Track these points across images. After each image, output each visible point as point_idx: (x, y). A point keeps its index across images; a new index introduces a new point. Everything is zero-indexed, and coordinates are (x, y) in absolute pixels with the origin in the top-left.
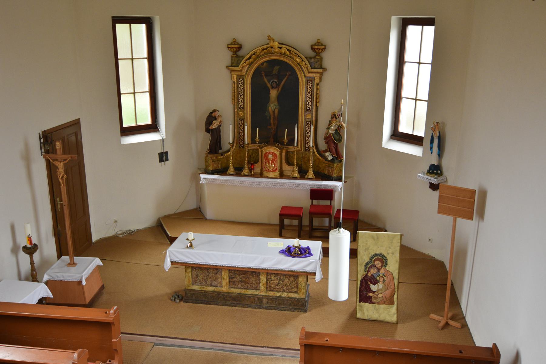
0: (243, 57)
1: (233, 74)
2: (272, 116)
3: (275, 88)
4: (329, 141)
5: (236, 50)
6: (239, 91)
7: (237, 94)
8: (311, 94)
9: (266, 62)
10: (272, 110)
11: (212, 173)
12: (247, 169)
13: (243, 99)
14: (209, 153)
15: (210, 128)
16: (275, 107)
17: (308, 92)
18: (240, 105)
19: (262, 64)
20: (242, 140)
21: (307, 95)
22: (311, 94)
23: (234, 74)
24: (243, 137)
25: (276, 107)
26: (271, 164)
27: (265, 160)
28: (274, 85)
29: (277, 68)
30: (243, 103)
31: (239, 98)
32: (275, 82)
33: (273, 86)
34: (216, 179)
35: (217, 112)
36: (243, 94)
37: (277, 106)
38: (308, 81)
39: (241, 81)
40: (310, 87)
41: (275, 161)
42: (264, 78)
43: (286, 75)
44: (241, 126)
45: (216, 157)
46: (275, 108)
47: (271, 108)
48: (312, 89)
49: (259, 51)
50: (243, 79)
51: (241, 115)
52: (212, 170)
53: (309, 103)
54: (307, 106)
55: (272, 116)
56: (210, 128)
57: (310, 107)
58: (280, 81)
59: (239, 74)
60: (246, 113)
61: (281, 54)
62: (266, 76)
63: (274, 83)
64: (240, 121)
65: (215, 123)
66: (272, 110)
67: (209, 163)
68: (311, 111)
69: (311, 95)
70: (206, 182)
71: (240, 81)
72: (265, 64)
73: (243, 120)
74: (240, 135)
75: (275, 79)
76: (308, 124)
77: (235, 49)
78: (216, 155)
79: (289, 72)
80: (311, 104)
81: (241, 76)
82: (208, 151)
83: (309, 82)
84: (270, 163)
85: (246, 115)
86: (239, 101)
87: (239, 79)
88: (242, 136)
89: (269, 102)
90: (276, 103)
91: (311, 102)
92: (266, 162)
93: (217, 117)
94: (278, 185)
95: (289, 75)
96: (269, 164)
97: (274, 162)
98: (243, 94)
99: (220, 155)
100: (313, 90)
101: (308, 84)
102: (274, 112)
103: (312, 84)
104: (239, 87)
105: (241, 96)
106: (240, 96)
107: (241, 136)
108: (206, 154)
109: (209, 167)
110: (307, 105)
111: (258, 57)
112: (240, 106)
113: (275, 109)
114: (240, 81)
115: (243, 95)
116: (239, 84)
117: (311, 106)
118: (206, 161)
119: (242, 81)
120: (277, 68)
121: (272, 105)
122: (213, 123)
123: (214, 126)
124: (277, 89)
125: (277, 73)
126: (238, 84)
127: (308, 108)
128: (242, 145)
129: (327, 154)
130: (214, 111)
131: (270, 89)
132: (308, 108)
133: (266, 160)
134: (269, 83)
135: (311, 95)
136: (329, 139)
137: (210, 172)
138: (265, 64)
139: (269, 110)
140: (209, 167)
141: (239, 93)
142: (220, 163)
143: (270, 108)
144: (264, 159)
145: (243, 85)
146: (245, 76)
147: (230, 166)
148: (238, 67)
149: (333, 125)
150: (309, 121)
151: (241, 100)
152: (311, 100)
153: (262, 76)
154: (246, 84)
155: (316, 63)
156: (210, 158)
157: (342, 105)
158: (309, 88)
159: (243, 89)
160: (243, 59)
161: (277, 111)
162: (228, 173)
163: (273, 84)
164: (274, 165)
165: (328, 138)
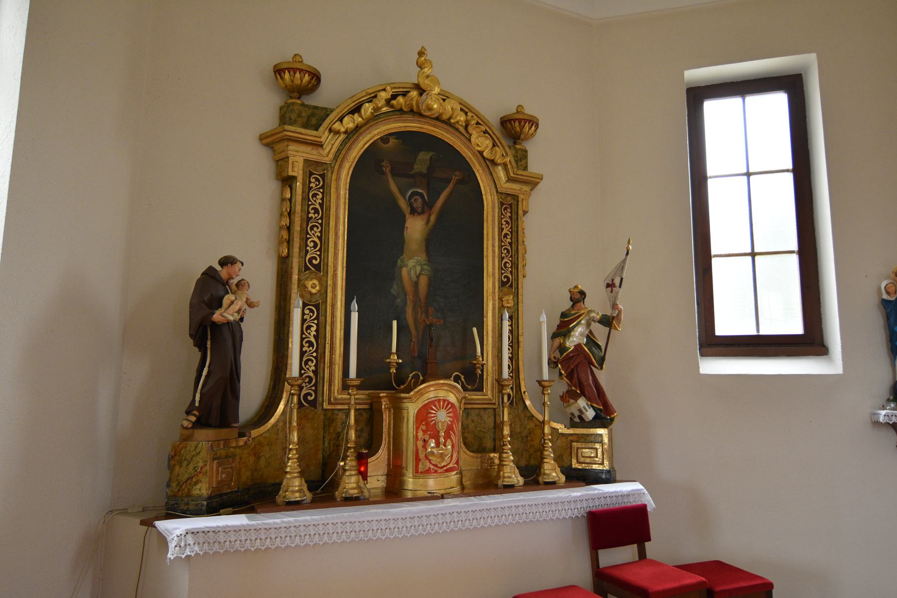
0: (327, 112)
1: (293, 153)
2: (410, 298)
3: (419, 214)
4: (577, 366)
5: (309, 82)
6: (309, 213)
7: (302, 220)
8: (510, 241)
9: (399, 135)
10: (410, 279)
11: (212, 510)
12: (353, 473)
13: (320, 238)
15: (217, 317)
16: (418, 269)
17: (503, 233)
18: (308, 257)
19: (385, 139)
20: (309, 377)
21: (502, 241)
22: (510, 241)
23: (294, 156)
24: (316, 366)
25: (422, 270)
26: (445, 445)
27: (420, 434)
28: (418, 204)
29: (424, 156)
30: (320, 250)
31: (308, 233)
32: (421, 195)
33: (415, 205)
34: (247, 530)
36: (320, 221)
37: (425, 267)
38: (502, 204)
39: (317, 179)
41: (454, 434)
42: (388, 181)
43: (448, 181)
46: (420, 274)
47: (409, 272)
48: (511, 228)
49: (384, 95)
50: (323, 176)
51: (314, 291)
52: (210, 498)
53: (507, 265)
54: (502, 274)
55: (411, 297)
56: (217, 317)
57: (510, 276)
58: (434, 195)
59: (313, 154)
60: (330, 282)
61: (438, 119)
62: (394, 174)
63: (418, 197)
65: (232, 302)
66: (410, 279)
67: (201, 464)
68: (511, 286)
69: (510, 244)
70: (196, 548)
71: (313, 180)
72: (393, 141)
73: (317, 306)
74: (304, 359)
75: (420, 188)
78: (224, 432)
79: (457, 173)
80: (511, 267)
81: (318, 164)
82: (193, 419)
83: (506, 209)
84: (442, 440)
85: (329, 289)
86: (307, 245)
87: (311, 174)
89: (401, 251)
90: (422, 257)
91: (511, 261)
92: (427, 437)
93: (234, 287)
94: (485, 515)
95: (459, 182)
96: (438, 444)
97: (453, 437)
98: (320, 221)
99: (235, 432)
100: (514, 229)
101: (502, 214)
102: (416, 285)
103: (511, 213)
104: (309, 200)
105: (315, 229)
106: (312, 229)
108: (186, 428)
109: (196, 483)
110: (502, 269)
111: (376, 117)
112: (310, 260)
113: (418, 277)
114: (313, 180)
115: (321, 224)
116: (310, 188)
117: (511, 272)
118: (175, 458)
119: (319, 183)
120: (424, 156)
121: (411, 263)
123: (225, 314)
124: (425, 217)
125: (425, 171)
126: (307, 188)
127: (505, 280)
128: (311, 395)
129: (582, 402)
130: (227, 261)
131: (407, 215)
132: (505, 277)
133: (425, 432)
134: (403, 195)
135: (510, 244)
136: (578, 360)
137: (205, 503)
138: (393, 141)
139: (401, 278)
140: (198, 487)
141: (309, 219)
143: (404, 271)
145: (323, 193)
148: (317, 130)
149: (583, 322)
151: (314, 241)
152: (511, 256)
153: (383, 173)
154: (333, 190)
156: (204, 446)
157: (627, 254)
158: (504, 223)
159: (321, 205)
160: (327, 115)
161: (423, 282)
162: (279, 499)
163: (415, 200)
164: (453, 446)
165: (572, 357)
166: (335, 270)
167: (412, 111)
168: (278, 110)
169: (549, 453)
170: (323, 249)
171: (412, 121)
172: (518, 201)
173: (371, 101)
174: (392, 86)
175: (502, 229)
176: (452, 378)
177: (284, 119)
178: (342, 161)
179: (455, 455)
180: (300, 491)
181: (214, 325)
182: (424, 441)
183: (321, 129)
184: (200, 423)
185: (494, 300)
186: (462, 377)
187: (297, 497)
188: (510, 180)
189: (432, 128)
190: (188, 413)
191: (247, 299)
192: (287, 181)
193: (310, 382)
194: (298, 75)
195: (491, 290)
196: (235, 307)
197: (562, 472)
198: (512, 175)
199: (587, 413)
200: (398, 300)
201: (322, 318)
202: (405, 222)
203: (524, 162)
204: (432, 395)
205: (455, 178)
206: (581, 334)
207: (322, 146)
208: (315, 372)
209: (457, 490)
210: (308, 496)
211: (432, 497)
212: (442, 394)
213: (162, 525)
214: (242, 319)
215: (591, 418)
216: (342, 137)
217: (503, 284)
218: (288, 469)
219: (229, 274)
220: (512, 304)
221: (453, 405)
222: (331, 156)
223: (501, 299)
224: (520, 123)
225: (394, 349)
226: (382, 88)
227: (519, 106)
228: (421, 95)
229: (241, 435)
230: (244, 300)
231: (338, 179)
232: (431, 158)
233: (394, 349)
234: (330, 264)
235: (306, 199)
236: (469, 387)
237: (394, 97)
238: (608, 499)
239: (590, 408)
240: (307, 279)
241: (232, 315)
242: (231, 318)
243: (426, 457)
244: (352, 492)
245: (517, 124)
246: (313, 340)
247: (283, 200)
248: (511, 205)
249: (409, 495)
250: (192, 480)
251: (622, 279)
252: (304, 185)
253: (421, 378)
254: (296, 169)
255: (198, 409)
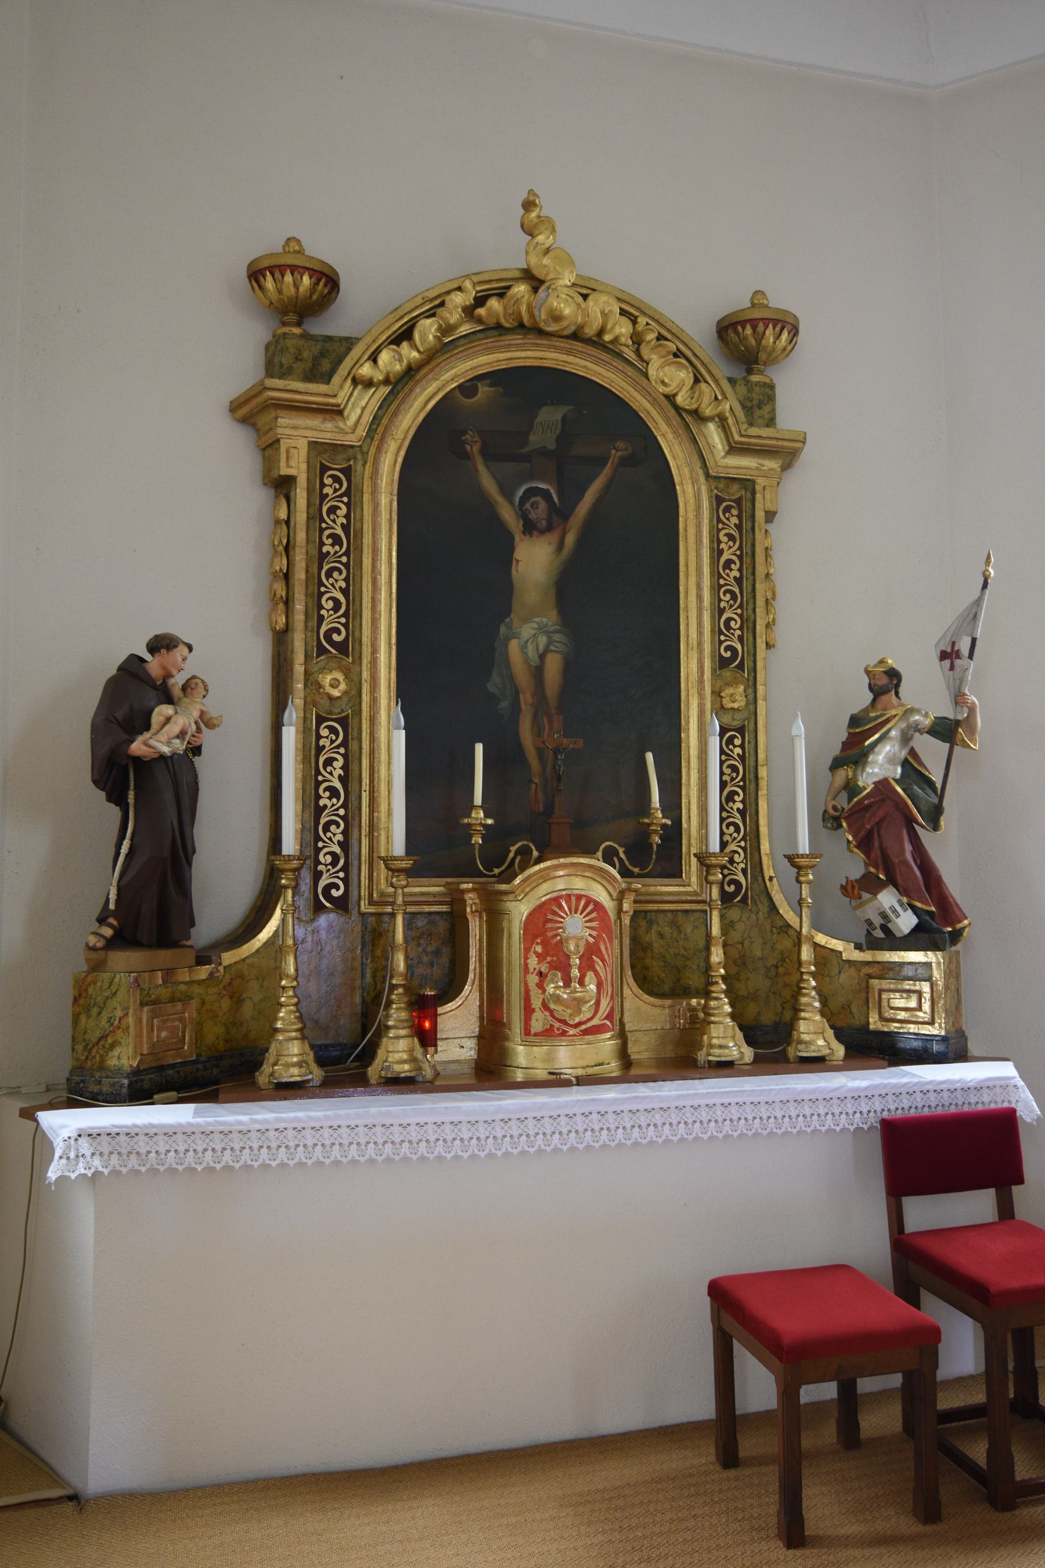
0: (349, 343)
1: (288, 431)
2: (526, 699)
3: (542, 532)
4: (879, 824)
5: (313, 289)
6: (322, 544)
7: (309, 559)
8: (738, 575)
9: (495, 377)
12: (403, 1032)
13: (345, 592)
14: (111, 944)
15: (137, 747)
16: (543, 640)
17: (723, 560)
18: (324, 628)
19: (468, 388)
21: (720, 576)
22: (738, 575)
23: (289, 437)
24: (345, 833)
25: (550, 642)
26: (581, 983)
27: (533, 962)
28: (539, 511)
29: (550, 416)
30: (346, 615)
31: (321, 584)
32: (546, 495)
33: (533, 515)
34: (188, 1132)
35: (183, 650)
36: (344, 559)
37: (557, 637)
38: (719, 500)
40: (731, 537)
41: (603, 960)
42: (477, 471)
43: (602, 461)
44: (329, 762)
45: (169, 973)
46: (547, 650)
47: (523, 648)
48: (740, 548)
49: (458, 300)
50: (347, 472)
51: (336, 693)
52: (136, 1072)
53: (732, 623)
54: (721, 642)
55: (530, 699)
56: (137, 747)
57: (739, 647)
58: (572, 494)
59: (325, 430)
60: (365, 675)
61: (576, 336)
62: (488, 456)
63: (538, 499)
64: (324, 732)
65: (168, 720)
66: (526, 661)
67: (119, 1013)
69: (739, 581)
70: (97, 1162)
71: (328, 481)
72: (484, 391)
73: (344, 722)
74: (323, 820)
75: (544, 480)
76: (733, 737)
77: (306, 279)
78: (164, 956)
79: (619, 444)
80: (741, 628)
81: (335, 448)
82: (108, 932)
83: (727, 509)
84: (575, 972)
86: (321, 607)
87: (324, 469)
88: (337, 833)
89: (506, 610)
90: (550, 618)
91: (741, 616)
92: (544, 968)
93: (177, 692)
94: (658, 1119)
95: (624, 462)
96: (567, 983)
97: (599, 966)
98: (344, 559)
99: (190, 957)
100: (747, 549)
101: (719, 520)
102: (538, 673)
103: (739, 516)
104: (322, 520)
105: (335, 574)
106: (329, 574)
107: (326, 828)
108: (93, 949)
109: (112, 1046)
110: (721, 633)
112: (328, 635)
113: (542, 657)
114: (328, 481)
115: (347, 565)
116: (323, 497)
117: (741, 639)
119: (341, 485)
120: (550, 416)
121: (527, 631)
122: (156, 718)
124: (553, 537)
125: (552, 446)
127: (728, 654)
129: (888, 898)
130: (161, 644)
131: (517, 538)
132: (727, 649)
133: (541, 957)
134: (508, 496)
135: (739, 581)
136: (881, 813)
137: (126, 1082)
138: (484, 391)
139: (507, 662)
140: (116, 1052)
141: (323, 557)
142: (190, 1013)
143: (514, 645)
144: (527, 950)
146: (365, 454)
147: (279, 1025)
148: (328, 382)
149: (893, 733)
150: (736, 723)
152: (741, 606)
153: (466, 456)
154: (366, 497)
155: (759, 407)
156: (123, 980)
157: (985, 586)
158: (725, 539)
159: (346, 528)
161: (553, 666)
162: (262, 1078)
163: (532, 506)
164: (600, 985)
165: (870, 806)
166: (375, 650)
167: (521, 325)
168: (262, 349)
169: (811, 1000)
170: (351, 615)
171: (522, 347)
172: (754, 492)
173: (433, 315)
174: (476, 279)
175: (721, 552)
176: (599, 854)
177: (273, 367)
178: (382, 440)
179: (604, 1003)
180: (299, 1065)
181: (137, 760)
182: (540, 974)
183: (336, 379)
184: (122, 940)
185: (701, 696)
186: (621, 850)
187: (294, 1074)
188: (734, 449)
189: (564, 357)
190: (101, 920)
191: (202, 714)
192: (283, 486)
193: (334, 864)
194: (288, 278)
195: (694, 677)
196: (174, 728)
197: (839, 1037)
198: (737, 438)
199: (899, 921)
200: (504, 704)
201: (353, 745)
202: (512, 549)
203: (766, 409)
204: (560, 885)
205: (615, 455)
206: (891, 760)
207: (340, 413)
208: (344, 845)
209: (613, 1067)
210: (316, 1074)
211: (556, 1081)
212: (579, 884)
213: (48, 1119)
214: (197, 750)
215: (906, 931)
216: (385, 390)
217: (723, 663)
218: (279, 1025)
219: (164, 668)
220: (743, 704)
221: (598, 906)
222: (362, 431)
223: (717, 694)
224: (754, 328)
225: (478, 799)
226: (455, 285)
227: (756, 293)
228: (535, 290)
229: (202, 959)
230: (196, 714)
231: (375, 474)
232: (564, 418)
233: (478, 799)
234: (366, 639)
235: (315, 518)
236: (636, 870)
237: (480, 301)
238: (932, 1096)
239: (905, 910)
240: (322, 670)
241: (168, 743)
242: (166, 750)
243: (545, 1006)
244: (397, 1068)
245: (749, 331)
246: (338, 785)
247: (277, 522)
248: (738, 501)
249: (519, 1076)
250: (105, 1042)
251: (974, 641)
252: (310, 491)
253: (535, 853)
254: (293, 463)
255: (115, 914)
